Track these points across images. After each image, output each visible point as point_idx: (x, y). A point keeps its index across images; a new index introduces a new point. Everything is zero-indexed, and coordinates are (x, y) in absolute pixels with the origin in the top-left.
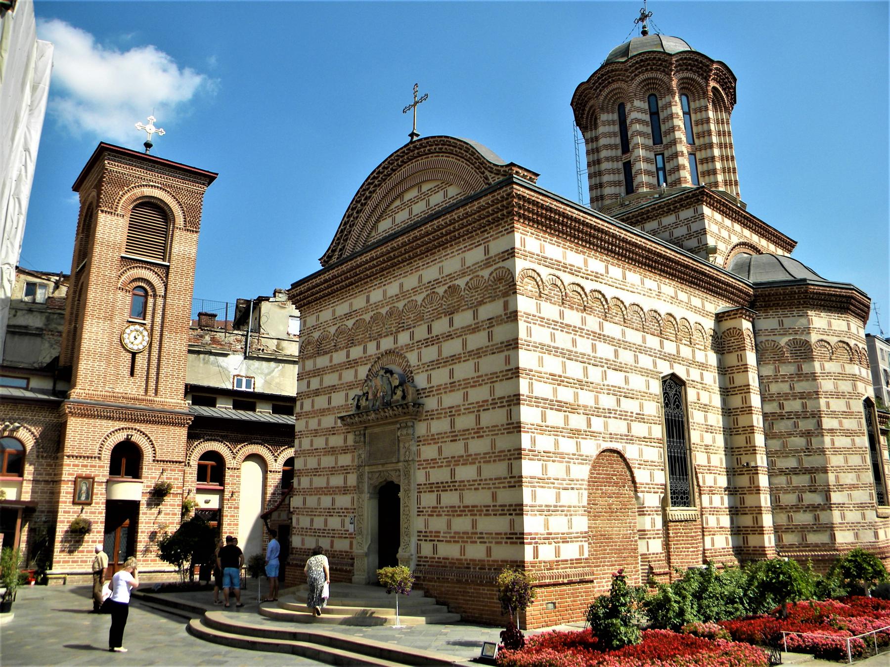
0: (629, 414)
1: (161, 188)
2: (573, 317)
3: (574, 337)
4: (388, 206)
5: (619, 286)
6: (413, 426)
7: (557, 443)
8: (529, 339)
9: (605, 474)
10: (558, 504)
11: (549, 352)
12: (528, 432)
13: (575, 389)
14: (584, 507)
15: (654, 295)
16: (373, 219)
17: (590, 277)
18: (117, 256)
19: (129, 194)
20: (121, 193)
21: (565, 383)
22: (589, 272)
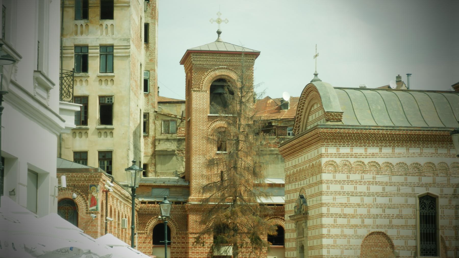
0: (391, 215)
1: (226, 68)
2: (355, 177)
3: (356, 186)
4: (311, 109)
5: (389, 156)
6: (306, 222)
7: (342, 231)
8: (328, 190)
9: (373, 242)
10: (342, 255)
11: (340, 194)
12: (326, 228)
13: (354, 208)
14: (357, 256)
15: (417, 155)
16: (307, 114)
17: (368, 157)
18: (205, 116)
19: (208, 77)
20: (203, 77)
21: (349, 206)
22: (368, 154)
